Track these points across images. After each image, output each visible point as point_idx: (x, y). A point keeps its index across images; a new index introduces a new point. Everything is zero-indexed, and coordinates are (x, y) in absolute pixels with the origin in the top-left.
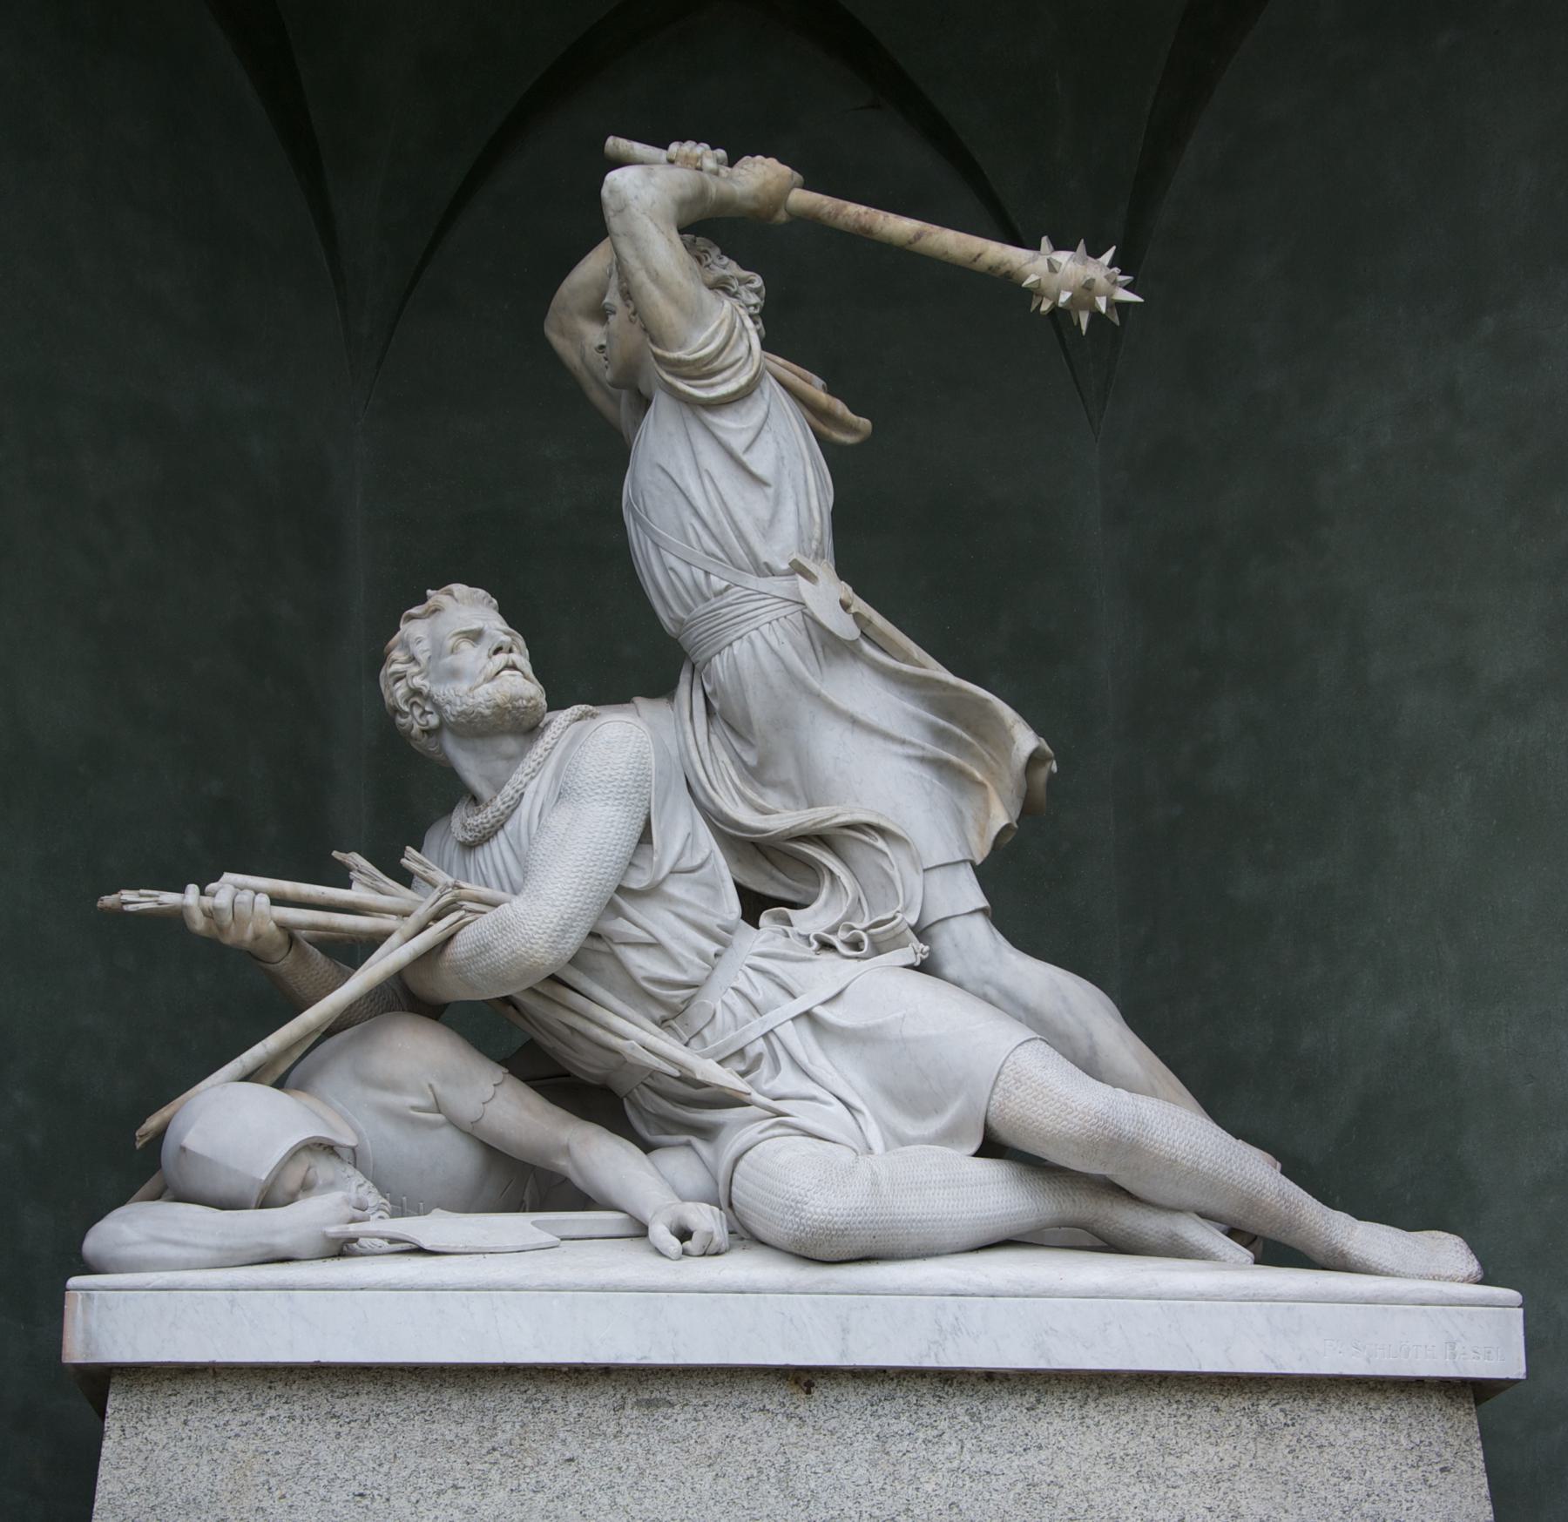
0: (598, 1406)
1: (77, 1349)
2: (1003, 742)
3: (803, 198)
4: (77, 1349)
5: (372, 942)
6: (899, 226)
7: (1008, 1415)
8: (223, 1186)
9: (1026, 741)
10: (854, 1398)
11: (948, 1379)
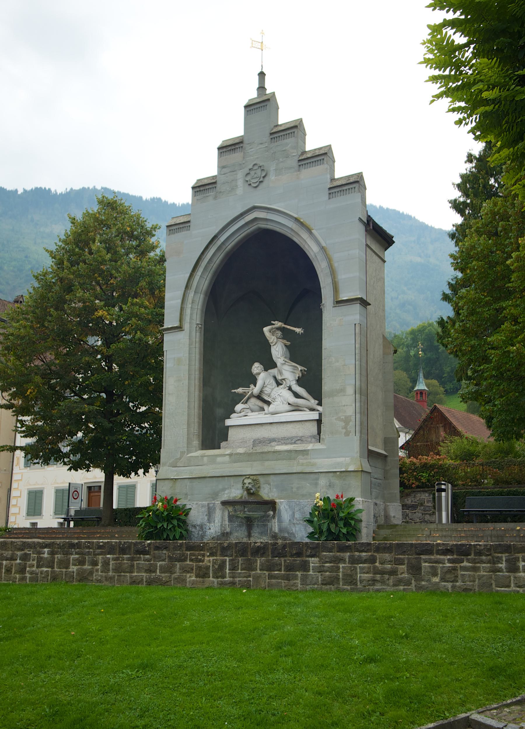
0: (258, 426)
1: (226, 425)
3: (283, 325)
4: (226, 425)
7: (285, 425)
10: (275, 424)
11: (281, 422)
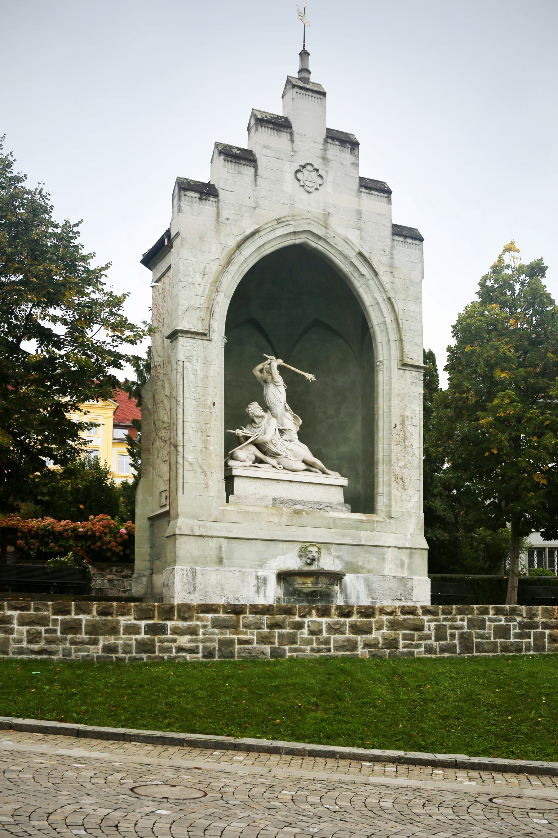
0: (275, 481)
2: (299, 421)
5: (250, 437)
6: (298, 371)
8: (241, 460)
9: (301, 422)
11: (302, 482)
